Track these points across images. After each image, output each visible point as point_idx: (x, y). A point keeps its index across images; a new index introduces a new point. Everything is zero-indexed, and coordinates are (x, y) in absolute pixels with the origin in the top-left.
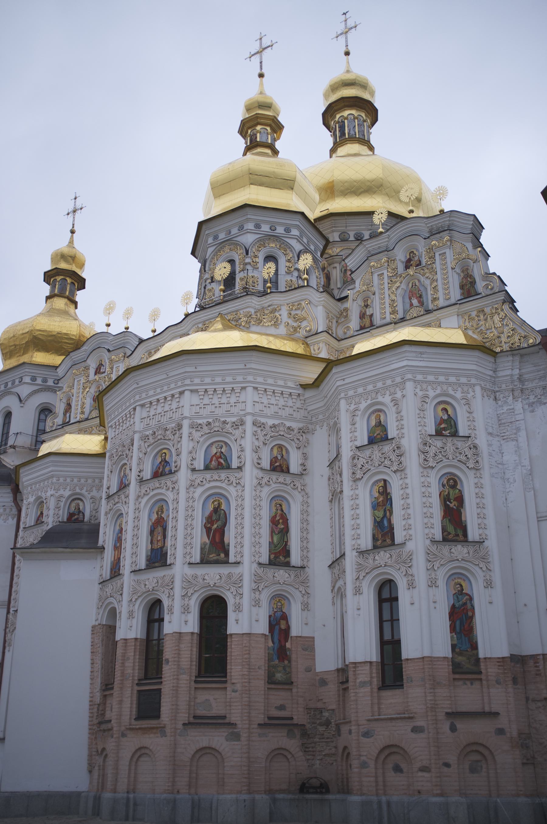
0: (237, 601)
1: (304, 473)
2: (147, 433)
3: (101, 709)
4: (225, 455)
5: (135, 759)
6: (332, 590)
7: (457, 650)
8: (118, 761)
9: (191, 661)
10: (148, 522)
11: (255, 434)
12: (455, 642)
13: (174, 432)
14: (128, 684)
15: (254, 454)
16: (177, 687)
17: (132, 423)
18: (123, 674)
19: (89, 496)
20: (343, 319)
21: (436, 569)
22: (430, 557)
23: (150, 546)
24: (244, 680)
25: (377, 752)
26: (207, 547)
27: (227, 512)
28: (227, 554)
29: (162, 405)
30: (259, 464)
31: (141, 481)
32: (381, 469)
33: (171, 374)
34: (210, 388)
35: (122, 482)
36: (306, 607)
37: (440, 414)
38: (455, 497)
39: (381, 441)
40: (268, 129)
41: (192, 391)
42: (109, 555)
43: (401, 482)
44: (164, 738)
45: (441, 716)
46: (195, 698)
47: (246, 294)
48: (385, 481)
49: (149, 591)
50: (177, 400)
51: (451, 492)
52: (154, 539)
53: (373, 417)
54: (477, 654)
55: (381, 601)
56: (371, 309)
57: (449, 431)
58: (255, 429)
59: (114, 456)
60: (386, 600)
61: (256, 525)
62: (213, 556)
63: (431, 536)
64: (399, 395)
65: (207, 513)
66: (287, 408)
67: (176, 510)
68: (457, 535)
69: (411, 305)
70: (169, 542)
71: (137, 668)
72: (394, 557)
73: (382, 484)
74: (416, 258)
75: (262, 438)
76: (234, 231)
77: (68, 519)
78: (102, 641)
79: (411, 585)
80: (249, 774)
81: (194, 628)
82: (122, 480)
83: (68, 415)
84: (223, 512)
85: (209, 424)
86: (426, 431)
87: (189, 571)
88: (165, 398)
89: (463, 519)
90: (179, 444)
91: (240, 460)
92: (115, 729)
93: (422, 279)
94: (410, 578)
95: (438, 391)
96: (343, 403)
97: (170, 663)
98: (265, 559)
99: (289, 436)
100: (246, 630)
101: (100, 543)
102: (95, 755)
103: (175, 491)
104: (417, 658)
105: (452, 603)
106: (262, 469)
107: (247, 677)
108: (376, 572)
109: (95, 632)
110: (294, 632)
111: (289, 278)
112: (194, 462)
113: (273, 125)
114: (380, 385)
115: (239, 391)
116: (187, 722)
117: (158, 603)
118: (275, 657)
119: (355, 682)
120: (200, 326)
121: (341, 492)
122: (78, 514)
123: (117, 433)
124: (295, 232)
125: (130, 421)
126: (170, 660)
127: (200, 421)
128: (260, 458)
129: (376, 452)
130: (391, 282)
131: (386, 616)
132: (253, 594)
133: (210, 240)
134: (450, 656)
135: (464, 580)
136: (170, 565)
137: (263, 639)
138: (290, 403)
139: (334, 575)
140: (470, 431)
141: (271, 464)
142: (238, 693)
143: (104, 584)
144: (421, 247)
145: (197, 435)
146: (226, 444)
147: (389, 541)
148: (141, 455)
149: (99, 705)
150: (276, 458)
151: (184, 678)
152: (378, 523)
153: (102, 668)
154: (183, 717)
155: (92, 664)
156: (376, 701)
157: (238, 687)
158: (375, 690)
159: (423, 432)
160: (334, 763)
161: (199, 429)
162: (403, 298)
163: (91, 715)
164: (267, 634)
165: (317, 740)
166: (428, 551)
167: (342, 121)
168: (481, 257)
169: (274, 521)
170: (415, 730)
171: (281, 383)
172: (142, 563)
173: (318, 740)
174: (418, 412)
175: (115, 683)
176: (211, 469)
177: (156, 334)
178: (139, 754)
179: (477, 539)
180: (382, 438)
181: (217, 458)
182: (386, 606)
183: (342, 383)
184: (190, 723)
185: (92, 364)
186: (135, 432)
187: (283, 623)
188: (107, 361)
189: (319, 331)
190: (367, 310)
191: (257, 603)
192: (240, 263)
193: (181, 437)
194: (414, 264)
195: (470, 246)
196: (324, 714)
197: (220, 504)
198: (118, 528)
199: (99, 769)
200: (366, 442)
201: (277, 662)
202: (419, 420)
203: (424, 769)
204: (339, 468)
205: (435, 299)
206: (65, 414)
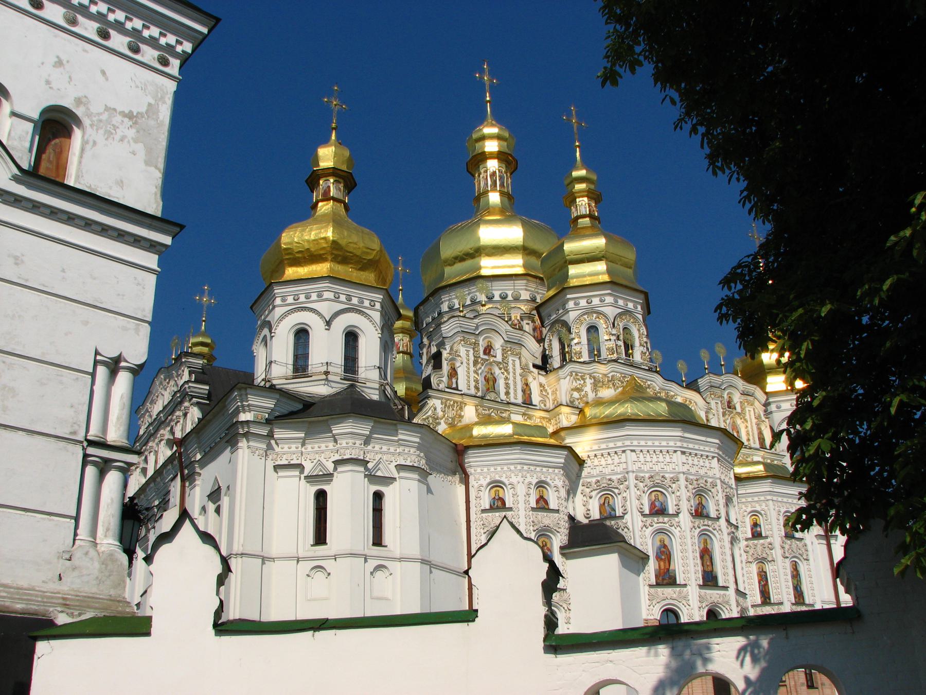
2: (691, 477)
17: (668, 459)
35: (652, 505)
48: (796, 562)
52: (705, 562)
83: (454, 380)
130: (724, 414)
147: (802, 601)
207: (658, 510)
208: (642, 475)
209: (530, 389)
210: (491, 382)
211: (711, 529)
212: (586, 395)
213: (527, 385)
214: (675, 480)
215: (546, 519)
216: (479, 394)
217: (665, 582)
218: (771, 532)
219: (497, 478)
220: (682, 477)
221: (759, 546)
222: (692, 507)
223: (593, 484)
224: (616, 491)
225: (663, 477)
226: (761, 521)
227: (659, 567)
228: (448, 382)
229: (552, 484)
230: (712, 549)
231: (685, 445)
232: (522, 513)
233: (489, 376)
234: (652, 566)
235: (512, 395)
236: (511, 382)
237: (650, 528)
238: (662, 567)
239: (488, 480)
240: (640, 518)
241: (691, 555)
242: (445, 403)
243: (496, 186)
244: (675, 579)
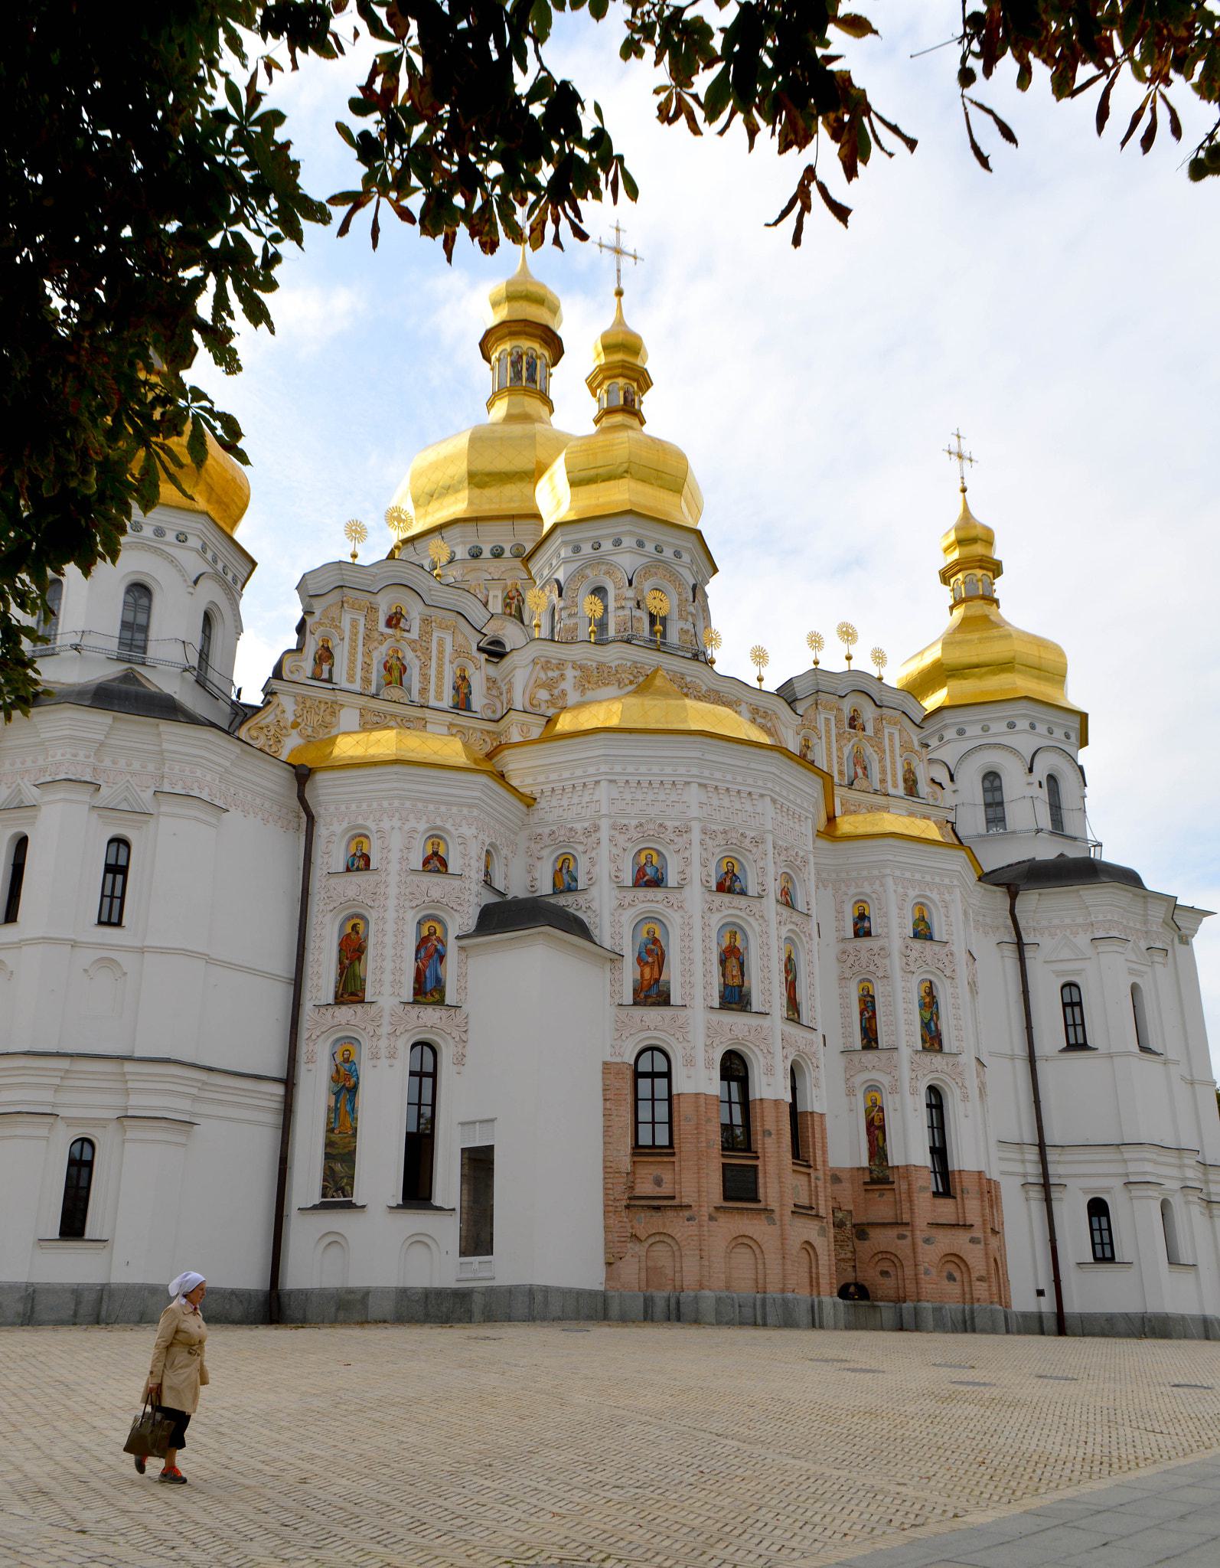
2: (714, 827)
17: (674, 798)
33: (753, 765)
48: (931, 982)
52: (728, 972)
64: (947, 897)
69: (856, 773)
73: (928, 984)
76: (668, 553)
79: (965, 1098)
83: (326, 667)
93: (869, 751)
96: (890, 881)
114: (928, 878)
120: (629, 664)
127: (780, 843)
146: (791, 877)
148: (704, 855)
149: (628, 1174)
170: (973, 1241)
198: (643, 935)
203: (980, 1279)
207: (649, 879)
208: (625, 822)
209: (469, 686)
210: (395, 672)
211: (744, 916)
212: (564, 693)
213: (464, 678)
214: (683, 831)
215: (435, 886)
216: (373, 690)
218: (885, 930)
219: (360, 821)
220: (696, 827)
221: (863, 952)
222: (710, 876)
223: (545, 837)
224: (581, 848)
225: (661, 825)
226: (872, 912)
227: (642, 975)
228: (313, 673)
229: (455, 833)
230: (746, 948)
231: (706, 773)
232: (393, 879)
233: (394, 661)
234: (629, 973)
235: (432, 693)
236: (433, 672)
238: (647, 976)
239: (345, 825)
240: (616, 892)
241: (698, 957)
242: (302, 701)
243: (521, 379)
244: (669, 996)
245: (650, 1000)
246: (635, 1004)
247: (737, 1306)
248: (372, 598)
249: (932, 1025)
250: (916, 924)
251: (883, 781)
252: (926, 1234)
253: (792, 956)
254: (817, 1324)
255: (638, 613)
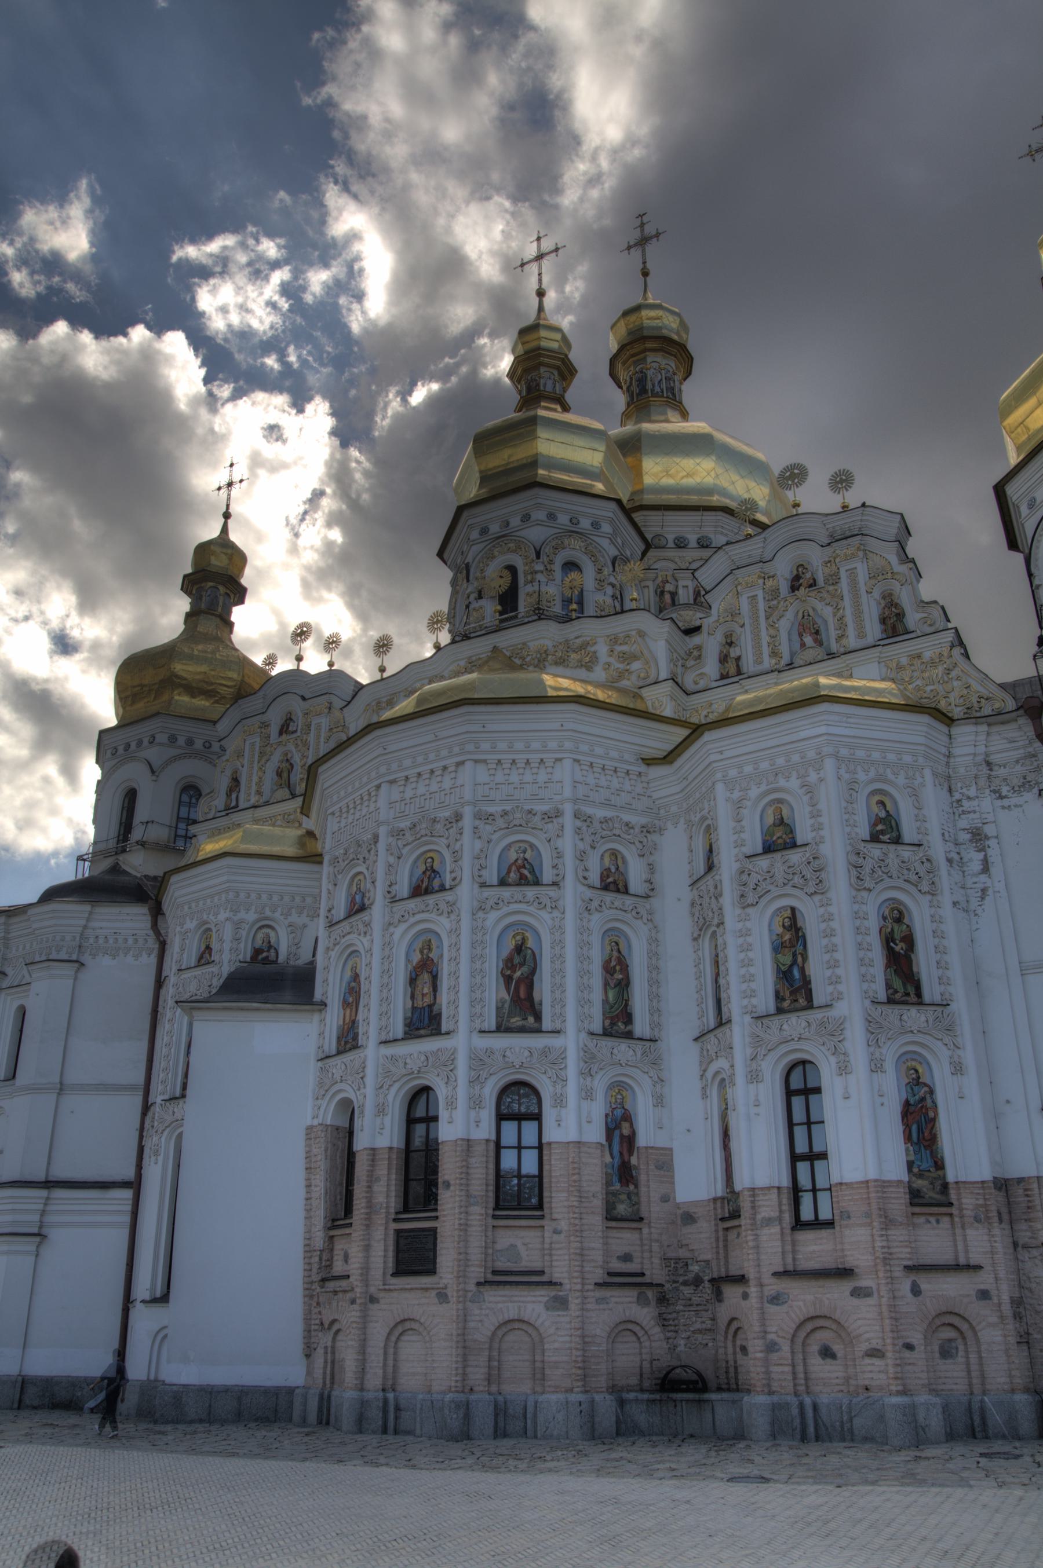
0: (559, 1091)
1: (651, 894)
2: (402, 825)
3: (324, 1258)
4: (530, 864)
5: (393, 1338)
6: (702, 1076)
7: (915, 1170)
8: (365, 1340)
9: (487, 1185)
10: (406, 966)
11: (578, 831)
12: (912, 1158)
13: (449, 826)
14: (380, 1219)
15: (578, 862)
16: (467, 1225)
17: (372, 809)
18: (370, 1205)
19: (286, 922)
20: (691, 663)
21: (881, 1044)
22: (873, 1029)
23: (410, 1003)
24: (571, 1215)
25: (794, 1326)
26: (507, 1006)
27: (537, 952)
28: (538, 1017)
29: (427, 782)
30: (585, 878)
31: (394, 900)
32: (788, 890)
34: (507, 757)
35: (353, 901)
36: (659, 1101)
37: (875, 809)
38: (903, 934)
39: (785, 848)
40: (556, 373)
41: (476, 761)
42: (334, 1017)
43: (822, 910)
44: (444, 1305)
45: (898, 1272)
46: (494, 1242)
47: (536, 617)
48: (793, 910)
49: (413, 1073)
50: (453, 775)
51: (896, 928)
52: (418, 993)
53: (770, 811)
54: (944, 1177)
55: (790, 1093)
56: (737, 649)
57: (888, 836)
58: (578, 823)
59: (340, 860)
60: (798, 1092)
61: (583, 973)
62: (516, 1021)
63: (871, 994)
64: (813, 777)
65: (505, 953)
66: (623, 794)
67: (456, 946)
68: (908, 994)
69: (803, 645)
70: (444, 998)
71: (393, 1194)
72: (813, 1027)
73: (788, 913)
74: (808, 575)
75: (588, 839)
76: (515, 521)
77: (252, 958)
78: (326, 1151)
79: (844, 1069)
80: (584, 1362)
81: (490, 1133)
82: (354, 899)
83: (234, 796)
84: (529, 952)
85: (505, 813)
86: (857, 834)
87: (483, 1043)
88: (432, 772)
89: (915, 969)
90: (458, 844)
91: (555, 872)
92: (358, 1290)
93: (819, 606)
94: (842, 1057)
95: (872, 774)
96: (720, 787)
97: (452, 1188)
98: (597, 1027)
99: (627, 837)
100: (572, 1136)
101: (318, 996)
102: (315, 1330)
103: (453, 917)
104: (857, 1183)
105: (904, 1096)
106: (590, 887)
107: (577, 1210)
108: (784, 1049)
109: (313, 1135)
110: (642, 1141)
111: (600, 597)
112: (484, 872)
113: (563, 368)
114: (780, 761)
115: (551, 764)
116: (482, 1280)
117: (425, 1091)
118: (615, 1179)
119: (754, 1219)
121: (721, 924)
122: (268, 951)
123: (343, 824)
124: (606, 528)
125: (368, 806)
126: (452, 1182)
127: (491, 809)
128: (587, 870)
129: (777, 862)
131: (799, 1116)
132: (582, 1080)
133: (475, 535)
134: (906, 1178)
135: (920, 1063)
136: (448, 1033)
137: (599, 1151)
138: (627, 786)
139: (705, 1053)
140: (920, 836)
141: (602, 880)
142: (562, 1235)
143: (328, 1061)
144: (816, 557)
145: (486, 829)
146: (532, 846)
150: (608, 870)
151: (477, 1211)
152: (784, 973)
153: (326, 1193)
154: (477, 1272)
155: (308, 1186)
156: (789, 1248)
157: (563, 1225)
158: (788, 1231)
159: (853, 835)
160: (710, 1344)
161: (489, 821)
162: (789, 634)
163: (307, 1267)
164: (604, 1142)
165: (679, 1307)
166: (869, 1018)
167: (641, 372)
168: (912, 575)
169: (608, 969)
170: (857, 1293)
171: (614, 754)
172: (399, 1030)
173: (682, 1308)
174: (844, 804)
175: (354, 1218)
176: (510, 885)
177: (385, 675)
178: (400, 1329)
179: (937, 999)
180: (785, 843)
181: (518, 869)
182: (798, 1102)
183: (719, 757)
184: (487, 1283)
185: (275, 717)
186: (379, 824)
187: (625, 1125)
188: (300, 714)
189: (661, 679)
190: (732, 650)
191: (587, 1094)
192: (526, 574)
193: (461, 834)
194: (805, 584)
195: (894, 559)
196: (691, 1268)
197: (524, 940)
198: (348, 974)
199: (326, 1353)
200: (760, 850)
201: (617, 1186)
202: (847, 816)
204: (716, 887)
205: (840, 637)
206: (229, 795)
216: (265, 798)
217: (348, 1046)
228: (226, 805)
230: (442, 955)
237: (337, 947)
245: (348, 1046)
246: (339, 1053)
247: (392, 1409)
248: (264, 718)
249: (796, 973)
250: (767, 833)
251: (840, 637)
252: (770, 1290)
253: (530, 944)
254: (530, 1433)
255: (481, 602)
